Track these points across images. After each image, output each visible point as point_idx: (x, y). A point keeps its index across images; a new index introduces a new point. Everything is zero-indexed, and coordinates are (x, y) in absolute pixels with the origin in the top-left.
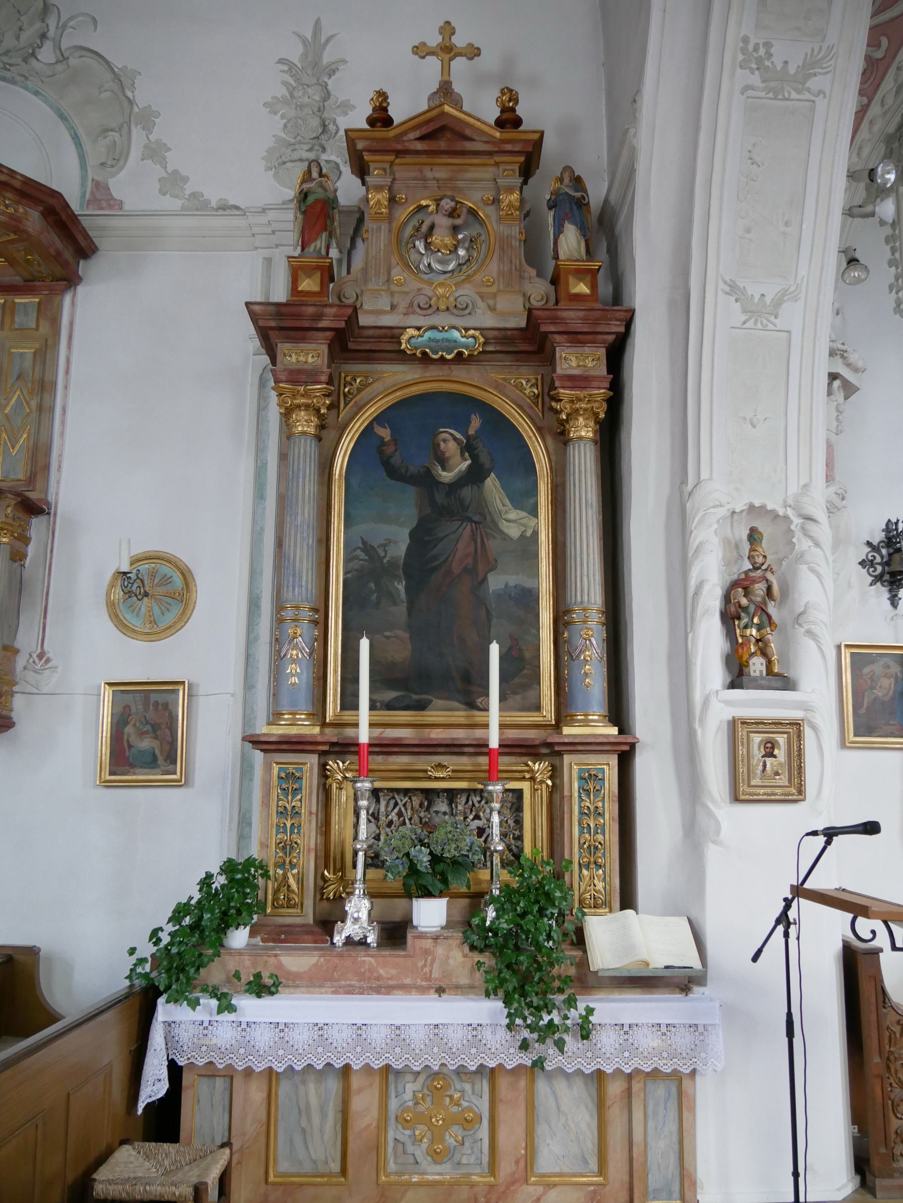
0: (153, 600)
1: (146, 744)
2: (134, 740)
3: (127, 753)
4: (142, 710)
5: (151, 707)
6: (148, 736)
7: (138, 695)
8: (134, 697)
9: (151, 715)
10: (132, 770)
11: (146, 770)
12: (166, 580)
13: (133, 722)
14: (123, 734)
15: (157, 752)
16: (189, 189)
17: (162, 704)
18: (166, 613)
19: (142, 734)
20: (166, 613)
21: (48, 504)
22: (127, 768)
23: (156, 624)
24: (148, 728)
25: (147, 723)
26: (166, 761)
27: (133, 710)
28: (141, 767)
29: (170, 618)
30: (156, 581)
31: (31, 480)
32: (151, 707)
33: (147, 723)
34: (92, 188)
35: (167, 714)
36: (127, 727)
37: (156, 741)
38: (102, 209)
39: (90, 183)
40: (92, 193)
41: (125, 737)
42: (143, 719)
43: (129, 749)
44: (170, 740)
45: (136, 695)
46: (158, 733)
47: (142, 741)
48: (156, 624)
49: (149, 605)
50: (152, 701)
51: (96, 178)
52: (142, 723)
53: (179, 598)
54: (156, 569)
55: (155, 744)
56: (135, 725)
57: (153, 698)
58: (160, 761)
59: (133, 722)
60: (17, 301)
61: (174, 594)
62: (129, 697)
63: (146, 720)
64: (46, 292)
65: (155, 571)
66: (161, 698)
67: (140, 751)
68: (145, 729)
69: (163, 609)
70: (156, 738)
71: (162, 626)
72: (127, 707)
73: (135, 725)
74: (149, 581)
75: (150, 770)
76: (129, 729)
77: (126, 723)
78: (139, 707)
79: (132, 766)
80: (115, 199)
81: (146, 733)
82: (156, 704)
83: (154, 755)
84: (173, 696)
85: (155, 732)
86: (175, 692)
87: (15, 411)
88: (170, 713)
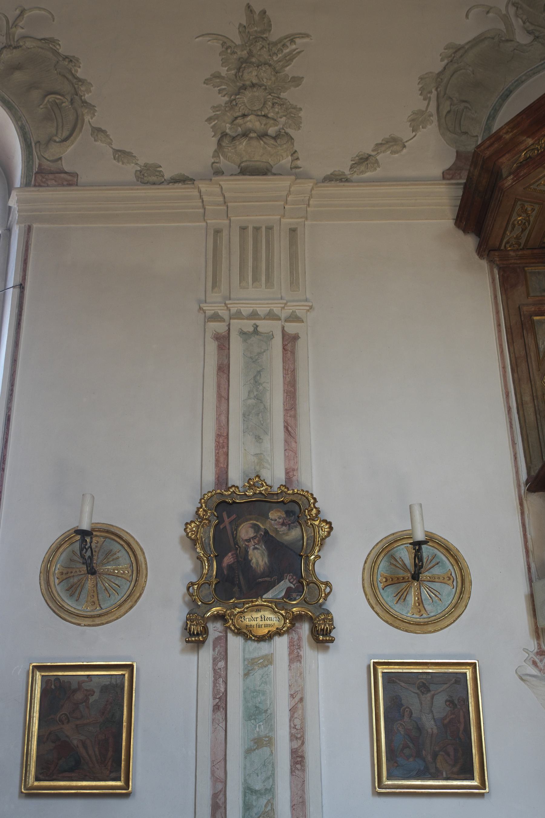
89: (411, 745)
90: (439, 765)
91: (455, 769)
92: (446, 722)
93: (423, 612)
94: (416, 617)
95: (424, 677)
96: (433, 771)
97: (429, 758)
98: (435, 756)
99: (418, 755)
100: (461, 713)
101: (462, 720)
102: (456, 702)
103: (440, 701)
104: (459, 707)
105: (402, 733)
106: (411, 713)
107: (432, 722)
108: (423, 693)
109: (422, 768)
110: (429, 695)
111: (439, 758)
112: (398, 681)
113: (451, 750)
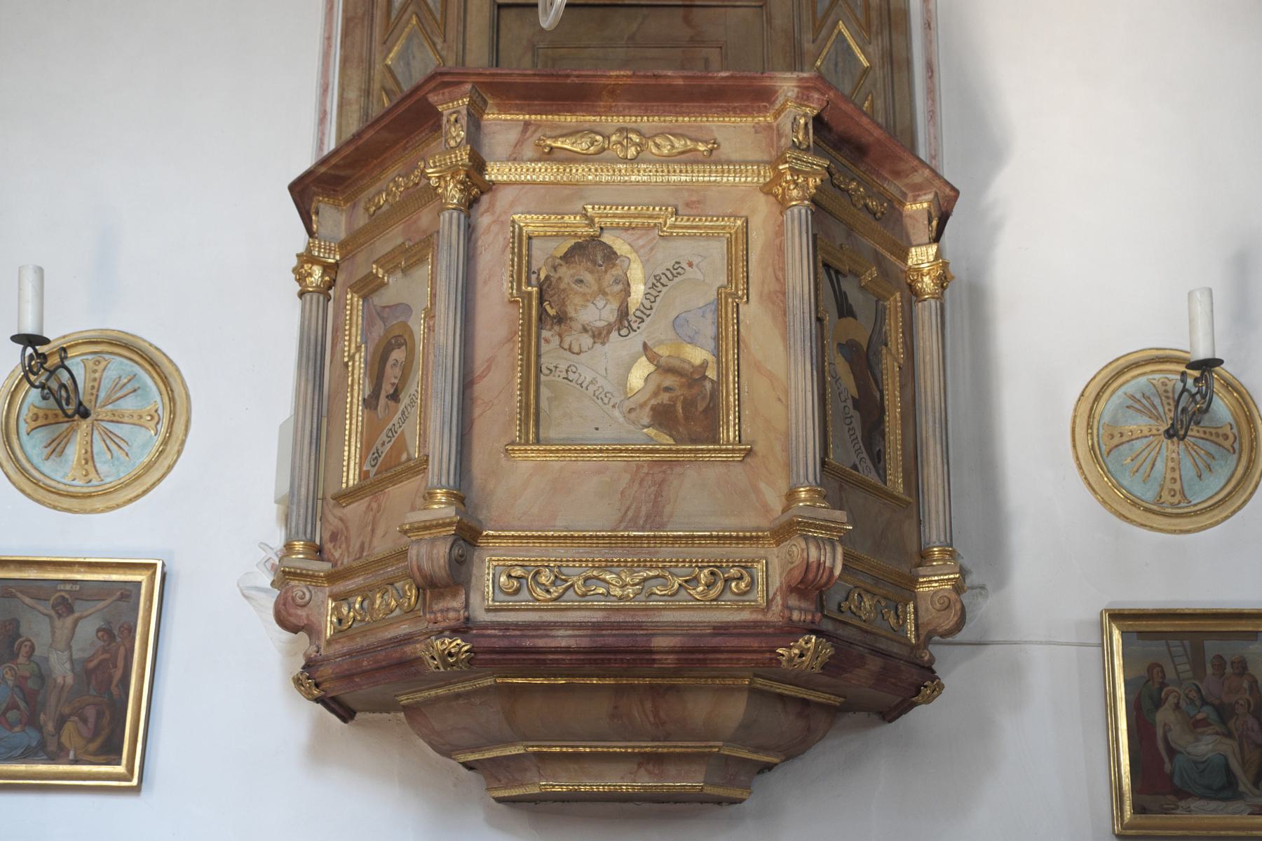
1: (1206, 746)
2: (1179, 737)
3: (1168, 767)
4: (1190, 674)
5: (1209, 670)
7: (1178, 643)
10: (1182, 804)
11: (1213, 805)
13: (1172, 700)
17: (1232, 663)
18: (1205, 474)
19: (1196, 725)
20: (1205, 474)
22: (1171, 797)
25: (1205, 702)
27: (1170, 674)
28: (1202, 797)
29: (1214, 484)
32: (1209, 670)
33: (1205, 702)
37: (1228, 741)
41: (1160, 732)
42: (1193, 694)
43: (1171, 760)
45: (1172, 643)
46: (1231, 724)
47: (1197, 740)
49: (1174, 455)
50: (1209, 655)
52: (1192, 702)
55: (1228, 747)
56: (1177, 707)
57: (1212, 648)
59: (1172, 700)
62: (1158, 647)
67: (1195, 763)
68: (1199, 716)
69: (1201, 465)
70: (1229, 735)
73: (1177, 707)
74: (1167, 408)
75: (1222, 804)
76: (1164, 716)
77: (1158, 704)
78: (1180, 668)
79: (1182, 794)
81: (1204, 723)
82: (1220, 662)
85: (1223, 720)
89: (22, 705)
90: (64, 739)
91: (93, 747)
92: (92, 665)
93: (92, 475)
94: (79, 486)
95: (68, 587)
96: (52, 747)
97: (50, 727)
98: (61, 722)
99: (32, 721)
100: (122, 651)
101: (121, 663)
102: (116, 632)
103: (88, 631)
104: (118, 640)
105: (10, 683)
106: (32, 648)
107: (68, 666)
108: (60, 616)
109: (34, 744)
110: (69, 620)
111: (69, 727)
112: (19, 595)
113: (91, 713)
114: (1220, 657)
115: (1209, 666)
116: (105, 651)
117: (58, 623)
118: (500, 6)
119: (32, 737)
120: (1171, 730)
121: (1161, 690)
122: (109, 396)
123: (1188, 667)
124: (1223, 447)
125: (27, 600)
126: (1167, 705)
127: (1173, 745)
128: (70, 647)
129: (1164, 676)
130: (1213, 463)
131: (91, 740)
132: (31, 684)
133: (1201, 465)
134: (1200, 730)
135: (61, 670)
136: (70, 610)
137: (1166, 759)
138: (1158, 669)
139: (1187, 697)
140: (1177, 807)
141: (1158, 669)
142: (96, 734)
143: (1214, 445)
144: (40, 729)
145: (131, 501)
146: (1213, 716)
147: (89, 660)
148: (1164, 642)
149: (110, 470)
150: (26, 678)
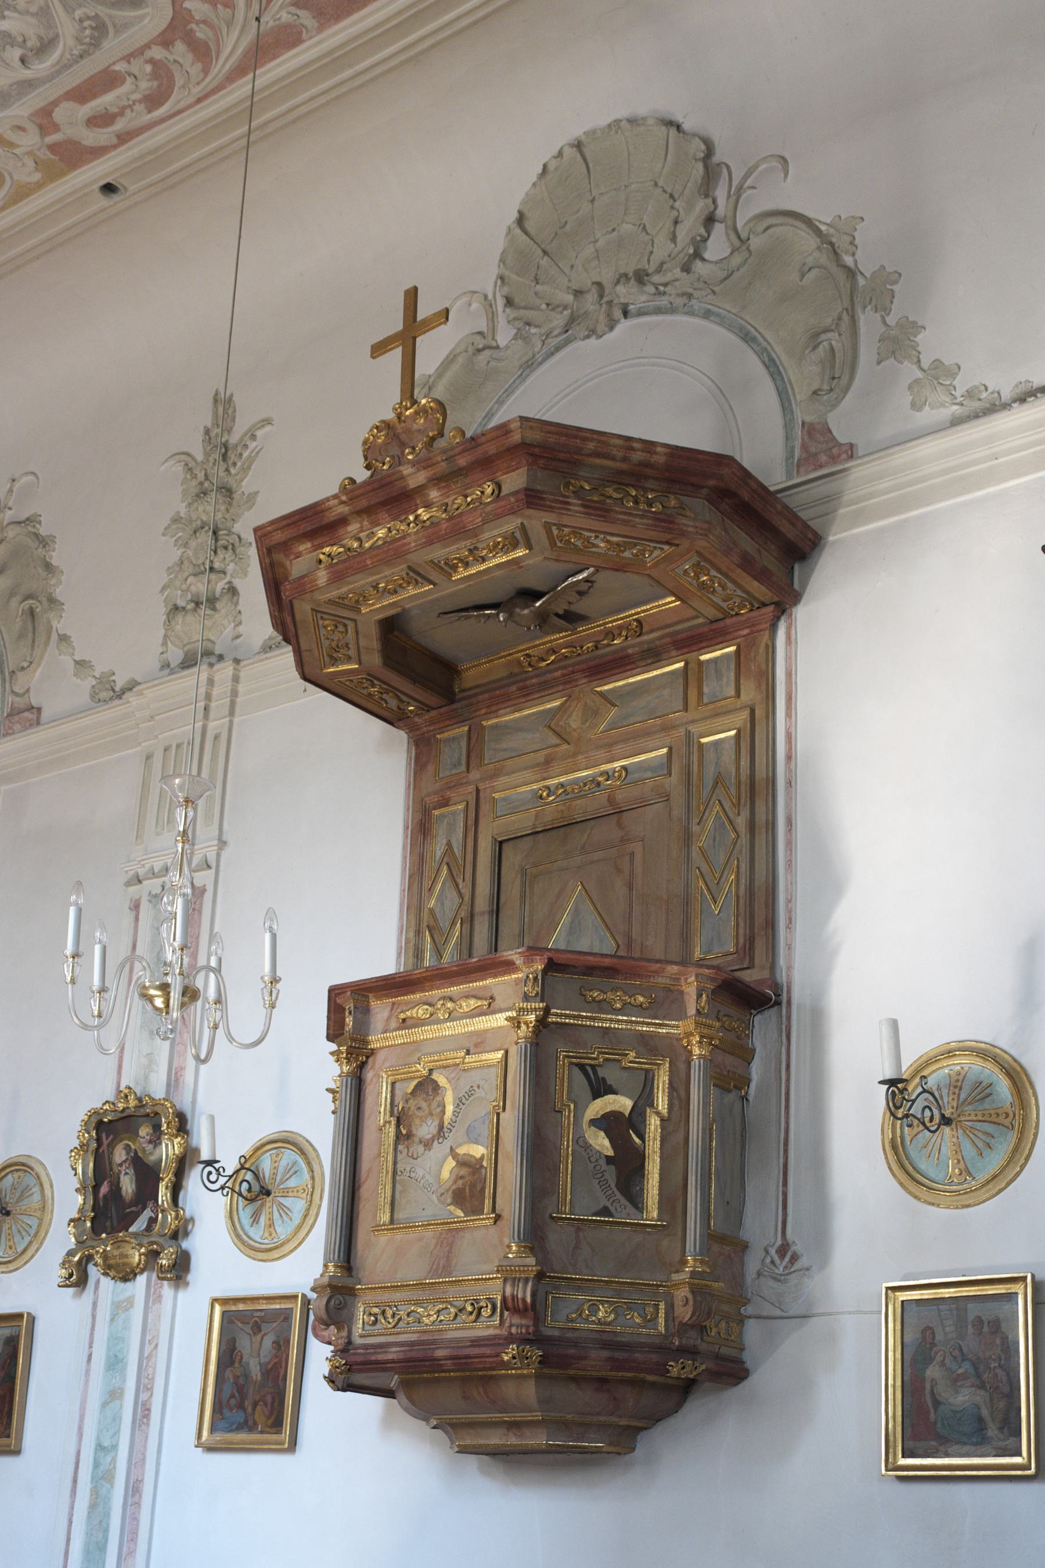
0: (960, 1131)
1: (963, 1398)
3: (932, 1416)
5: (970, 1330)
6: (968, 1383)
8: (939, 1309)
9: (971, 1343)
10: (941, 1448)
12: (983, 1091)
13: (939, 1358)
14: (924, 1380)
15: (985, 1413)
16: (961, 384)
18: (986, 1152)
19: (956, 1381)
20: (986, 1152)
21: (777, 987)
22: (934, 1443)
23: (970, 1175)
24: (967, 1366)
25: (964, 1358)
26: (1001, 1429)
27: (939, 1337)
28: (958, 1442)
30: (963, 1096)
31: (747, 949)
33: (964, 1358)
34: (803, 439)
35: (998, 1341)
36: (931, 1368)
37: (982, 1392)
38: (821, 467)
39: (798, 431)
40: (804, 446)
41: (928, 1386)
42: (956, 1353)
44: (1006, 1389)
47: (957, 1392)
48: (970, 1175)
50: (971, 1317)
51: (808, 419)
52: (955, 1358)
53: (1007, 1122)
54: (963, 1073)
56: (943, 1364)
57: (973, 1311)
58: (992, 1431)
60: (704, 658)
61: (998, 1115)
63: (963, 1354)
64: (746, 632)
65: (961, 1078)
66: (987, 1312)
67: (955, 1412)
68: (960, 1371)
69: (980, 1144)
70: (982, 1386)
71: (982, 1177)
72: (928, 1332)
76: (932, 1372)
77: (928, 1360)
78: (947, 1329)
80: (841, 445)
81: (965, 1376)
82: (979, 1321)
83: (980, 1420)
84: (1007, 1306)
86: (1011, 1297)
87: (714, 840)
88: (1005, 1339)
89: (237, 1394)
91: (270, 1422)
92: (270, 1366)
93: (274, 1235)
94: (268, 1243)
95: (259, 1314)
96: (250, 1423)
97: (250, 1409)
98: (255, 1405)
99: (241, 1406)
101: (283, 1365)
103: (268, 1342)
104: (283, 1348)
105: (231, 1380)
107: (258, 1368)
108: (255, 1334)
109: (242, 1421)
110: (259, 1337)
111: (258, 1408)
112: (236, 1321)
113: (269, 1399)
114: (979, 1317)
115: (970, 1326)
116: (276, 1356)
117: (254, 1339)
118: (501, 843)
119: (240, 1417)
120: (937, 1384)
121: (931, 1349)
122: (281, 1179)
123: (952, 1328)
124: (1003, 1125)
125: (240, 1324)
126: (935, 1363)
127: (938, 1397)
128: (259, 1355)
129: (934, 1338)
130: (992, 1142)
131: (269, 1418)
132: (241, 1381)
133: (980, 1144)
134: (959, 1384)
135: (256, 1372)
136: (260, 1330)
137: (932, 1411)
138: (930, 1331)
139: (952, 1355)
140: (937, 1451)
141: (930, 1331)
142: (271, 1414)
143: (992, 1125)
144: (244, 1410)
145: (292, 1251)
146: (971, 1370)
147: (269, 1363)
148: (935, 1307)
149: (283, 1230)
150: (238, 1377)
